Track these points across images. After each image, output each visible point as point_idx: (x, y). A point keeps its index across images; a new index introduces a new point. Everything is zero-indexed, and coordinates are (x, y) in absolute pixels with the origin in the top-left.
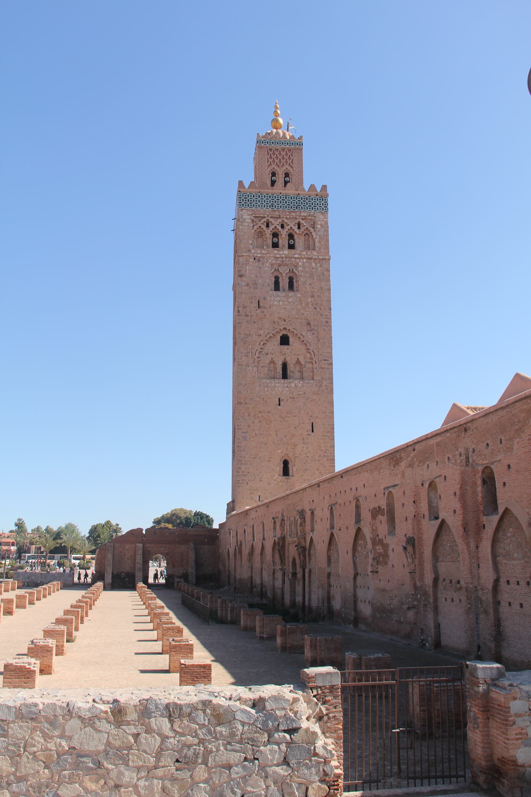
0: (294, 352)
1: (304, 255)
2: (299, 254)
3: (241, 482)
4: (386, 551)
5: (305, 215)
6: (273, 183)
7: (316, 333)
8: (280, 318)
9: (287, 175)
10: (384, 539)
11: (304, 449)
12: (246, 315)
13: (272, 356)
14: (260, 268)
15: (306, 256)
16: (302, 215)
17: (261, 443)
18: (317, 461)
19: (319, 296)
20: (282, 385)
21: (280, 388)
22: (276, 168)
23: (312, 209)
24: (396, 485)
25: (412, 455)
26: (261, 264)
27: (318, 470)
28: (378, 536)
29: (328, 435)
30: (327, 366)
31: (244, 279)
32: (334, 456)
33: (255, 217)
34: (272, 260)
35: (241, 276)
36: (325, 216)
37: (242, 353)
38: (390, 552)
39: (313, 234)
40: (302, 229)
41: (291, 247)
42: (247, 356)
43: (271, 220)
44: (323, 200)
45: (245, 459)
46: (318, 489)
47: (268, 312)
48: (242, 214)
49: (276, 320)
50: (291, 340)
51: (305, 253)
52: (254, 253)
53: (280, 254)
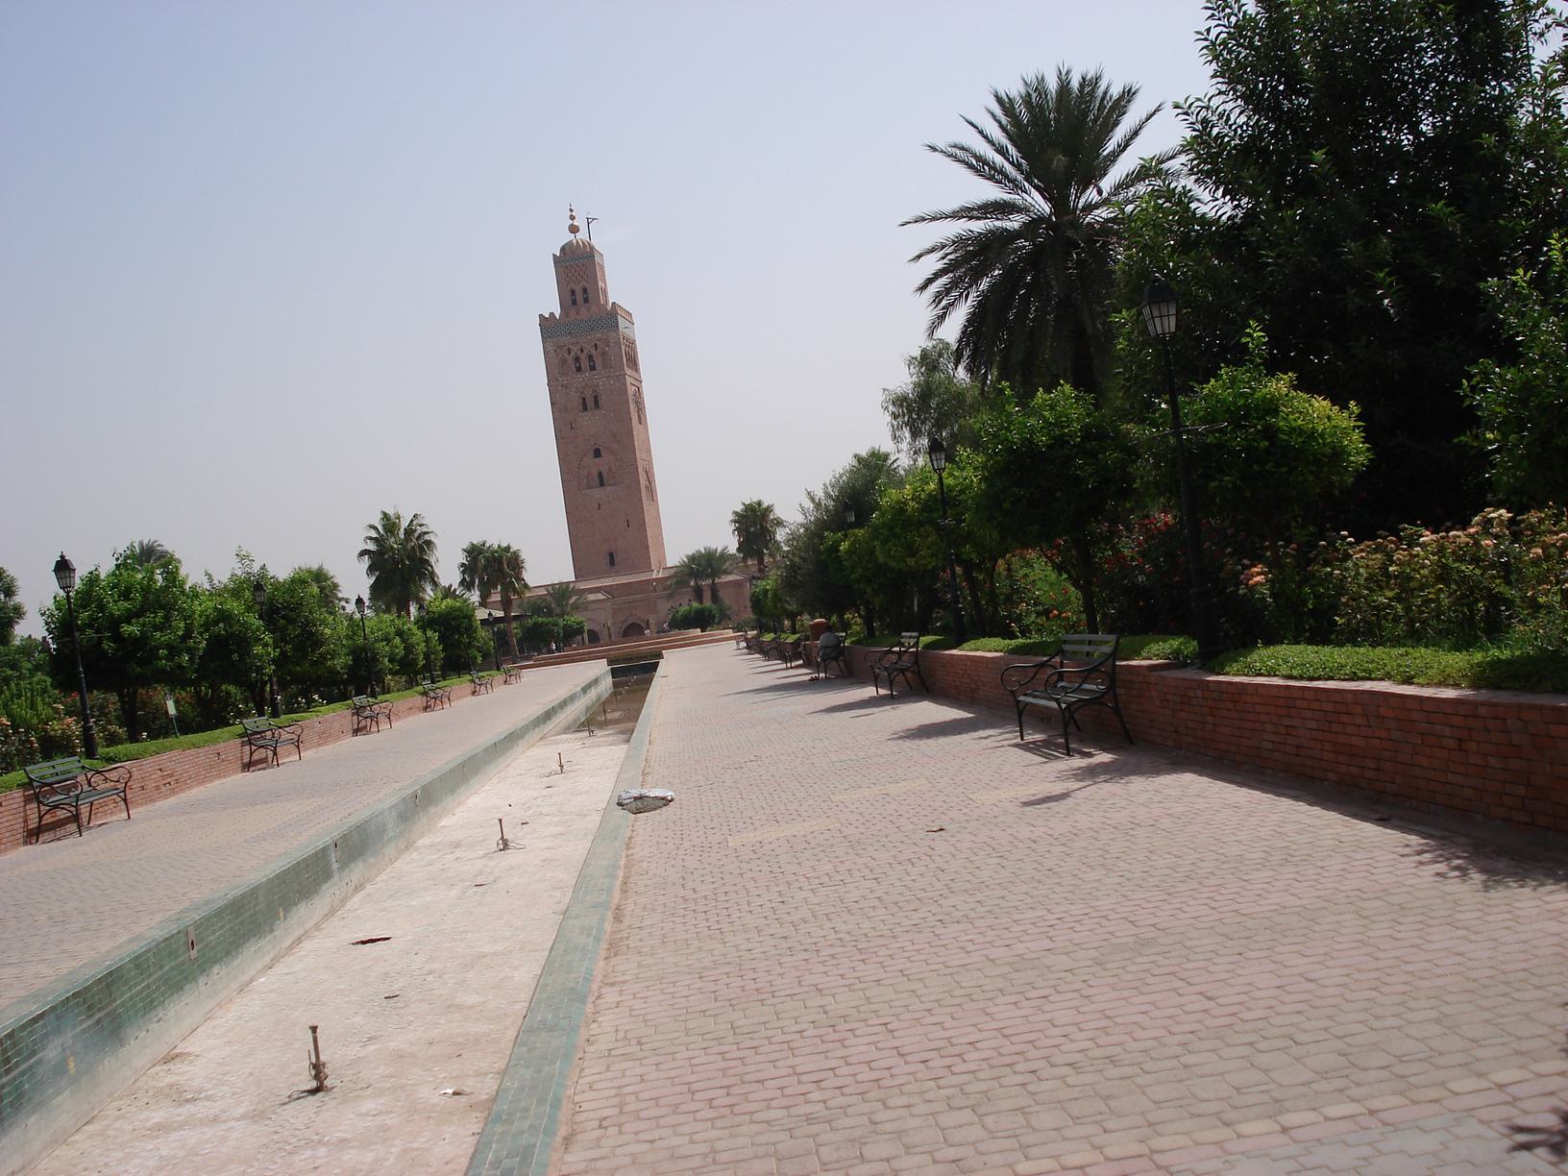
41: (593, 368)
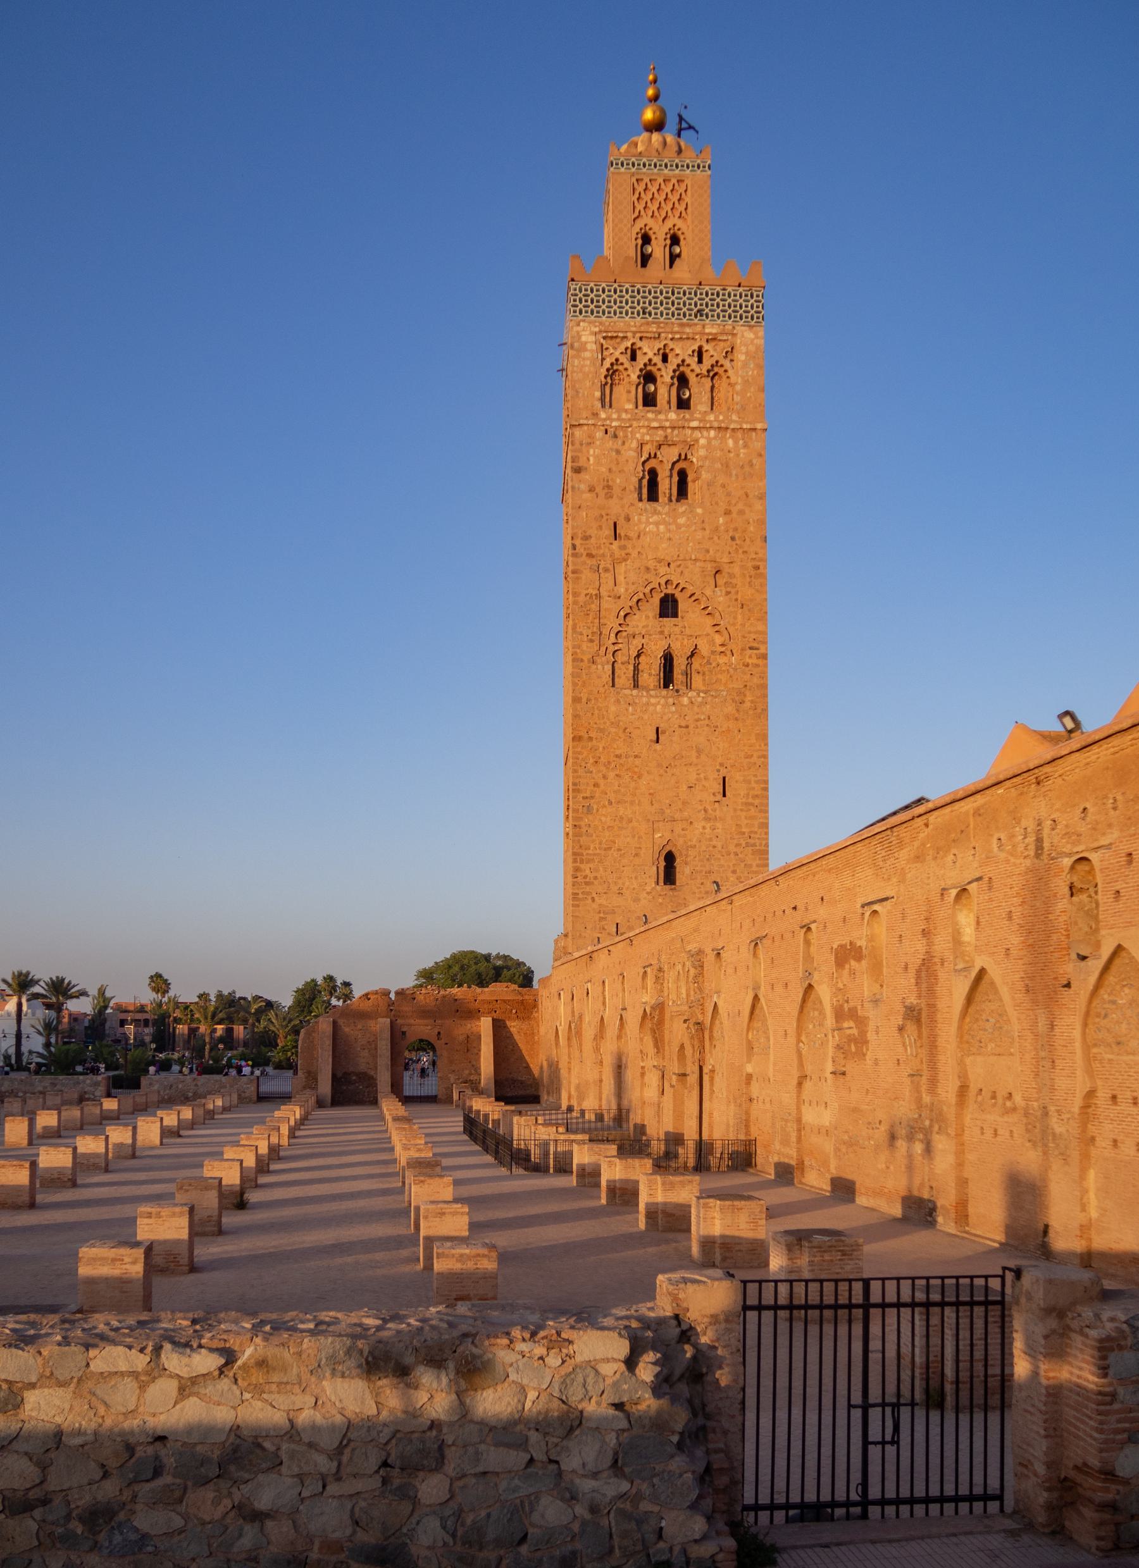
0: (688, 631)
1: (711, 422)
2: (700, 421)
3: (581, 896)
4: (863, 1033)
5: (714, 331)
6: (645, 260)
7: (733, 591)
8: (660, 561)
9: (675, 240)
10: (859, 1007)
11: (708, 831)
12: (590, 555)
13: (643, 641)
14: (618, 452)
15: (716, 425)
16: (707, 331)
17: (622, 818)
18: (732, 856)
19: (741, 512)
20: (662, 701)
21: (659, 707)
22: (651, 223)
23: (730, 317)
24: (886, 899)
25: (922, 835)
26: (620, 443)
27: (734, 872)
28: (847, 1002)
29: (757, 802)
30: (755, 661)
31: (584, 476)
32: (767, 845)
33: (604, 338)
34: (643, 435)
35: (578, 470)
36: (756, 334)
37: (581, 634)
38: (871, 1036)
39: (730, 373)
40: (707, 362)
41: (683, 404)
42: (592, 641)
43: (639, 344)
44: (752, 297)
45: (590, 852)
46: (730, 907)
47: (634, 547)
48: (578, 332)
49: (651, 564)
50: (681, 606)
51: (712, 417)
52: (605, 420)
53: (659, 421)
